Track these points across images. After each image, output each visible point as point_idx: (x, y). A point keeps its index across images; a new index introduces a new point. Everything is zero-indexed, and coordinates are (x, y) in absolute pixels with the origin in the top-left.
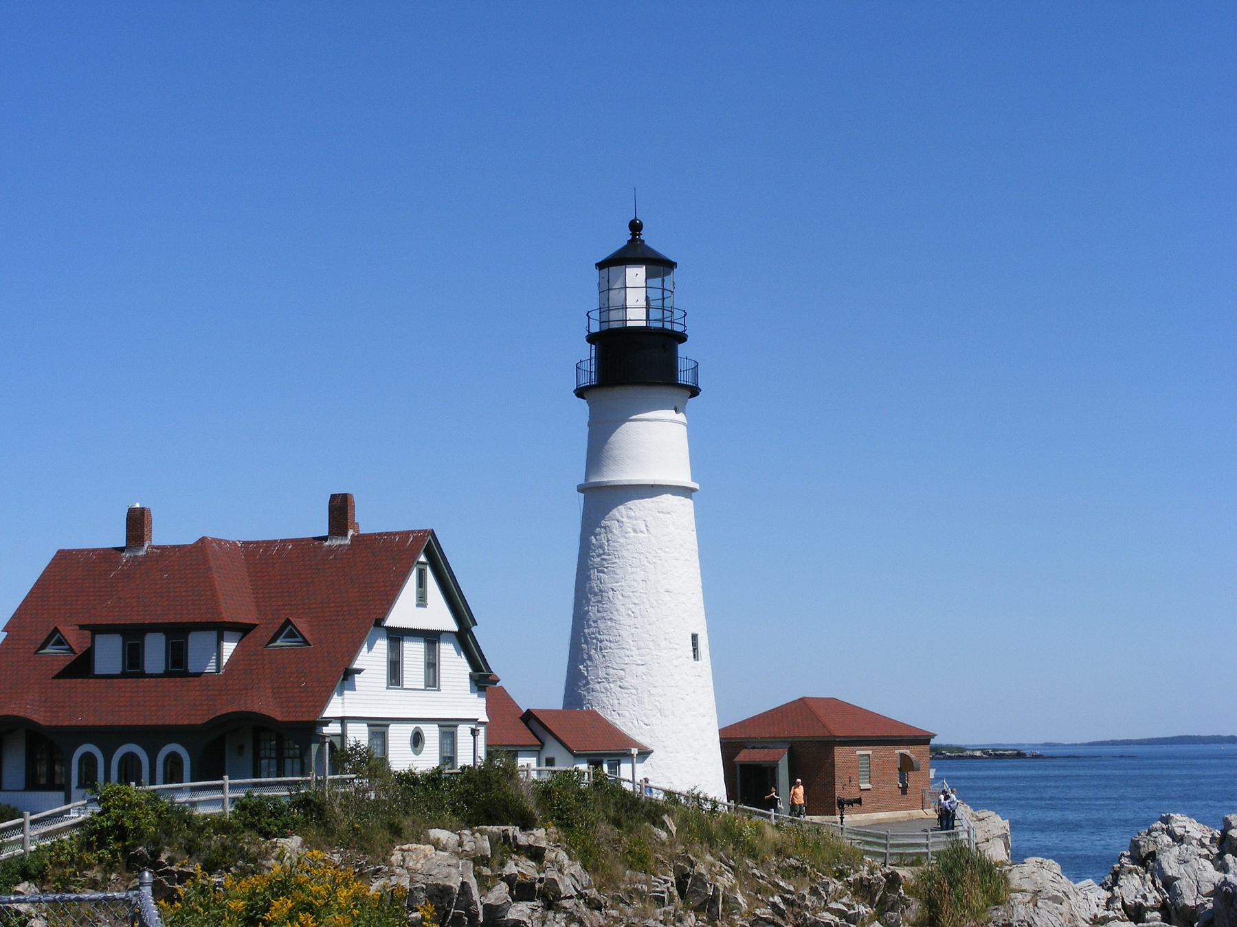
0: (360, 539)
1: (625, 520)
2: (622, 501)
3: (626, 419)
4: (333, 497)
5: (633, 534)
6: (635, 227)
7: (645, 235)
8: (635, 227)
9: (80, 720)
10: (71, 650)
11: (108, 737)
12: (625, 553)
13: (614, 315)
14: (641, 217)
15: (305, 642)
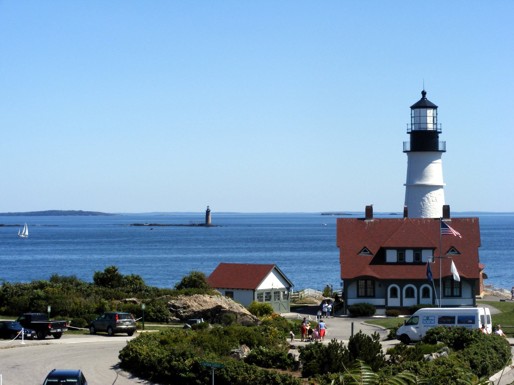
0: (454, 219)
1: (429, 197)
2: (429, 192)
3: (431, 162)
4: (444, 206)
5: (432, 202)
6: (424, 93)
7: (427, 96)
8: (424, 93)
9: (392, 277)
10: (371, 253)
11: (401, 282)
12: (430, 209)
13: (422, 126)
14: (426, 90)
15: (459, 253)
